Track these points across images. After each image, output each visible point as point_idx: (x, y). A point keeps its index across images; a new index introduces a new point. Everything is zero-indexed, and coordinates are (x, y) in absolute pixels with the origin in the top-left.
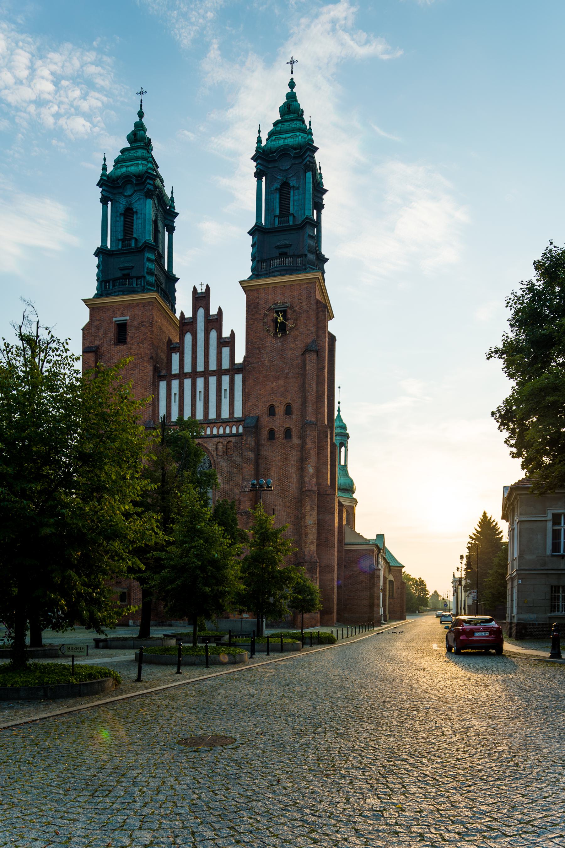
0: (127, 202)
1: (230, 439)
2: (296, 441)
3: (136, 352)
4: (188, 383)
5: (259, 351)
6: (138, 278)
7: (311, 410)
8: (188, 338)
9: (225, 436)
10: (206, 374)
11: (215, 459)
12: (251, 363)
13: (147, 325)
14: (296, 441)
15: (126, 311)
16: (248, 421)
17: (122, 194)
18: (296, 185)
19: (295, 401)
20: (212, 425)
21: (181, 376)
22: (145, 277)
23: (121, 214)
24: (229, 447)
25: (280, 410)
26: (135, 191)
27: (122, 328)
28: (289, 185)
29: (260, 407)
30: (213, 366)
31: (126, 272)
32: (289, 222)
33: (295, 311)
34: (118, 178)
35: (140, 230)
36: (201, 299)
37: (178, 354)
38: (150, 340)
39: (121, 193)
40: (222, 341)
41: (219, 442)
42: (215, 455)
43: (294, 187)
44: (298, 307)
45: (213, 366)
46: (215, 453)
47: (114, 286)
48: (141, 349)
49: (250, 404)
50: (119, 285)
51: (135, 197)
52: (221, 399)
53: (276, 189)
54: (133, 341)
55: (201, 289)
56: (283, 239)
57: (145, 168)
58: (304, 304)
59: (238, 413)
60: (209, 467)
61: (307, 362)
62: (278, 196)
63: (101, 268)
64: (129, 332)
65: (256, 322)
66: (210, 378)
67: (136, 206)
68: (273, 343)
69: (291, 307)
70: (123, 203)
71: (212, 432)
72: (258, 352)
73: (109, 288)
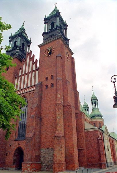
1: (33, 92)
2: (54, 87)
8: (24, 65)
18: (55, 22)
20: (28, 88)
21: (22, 75)
25: (49, 78)
42: (28, 98)
49: (40, 78)
59: (37, 83)
62: (51, 26)
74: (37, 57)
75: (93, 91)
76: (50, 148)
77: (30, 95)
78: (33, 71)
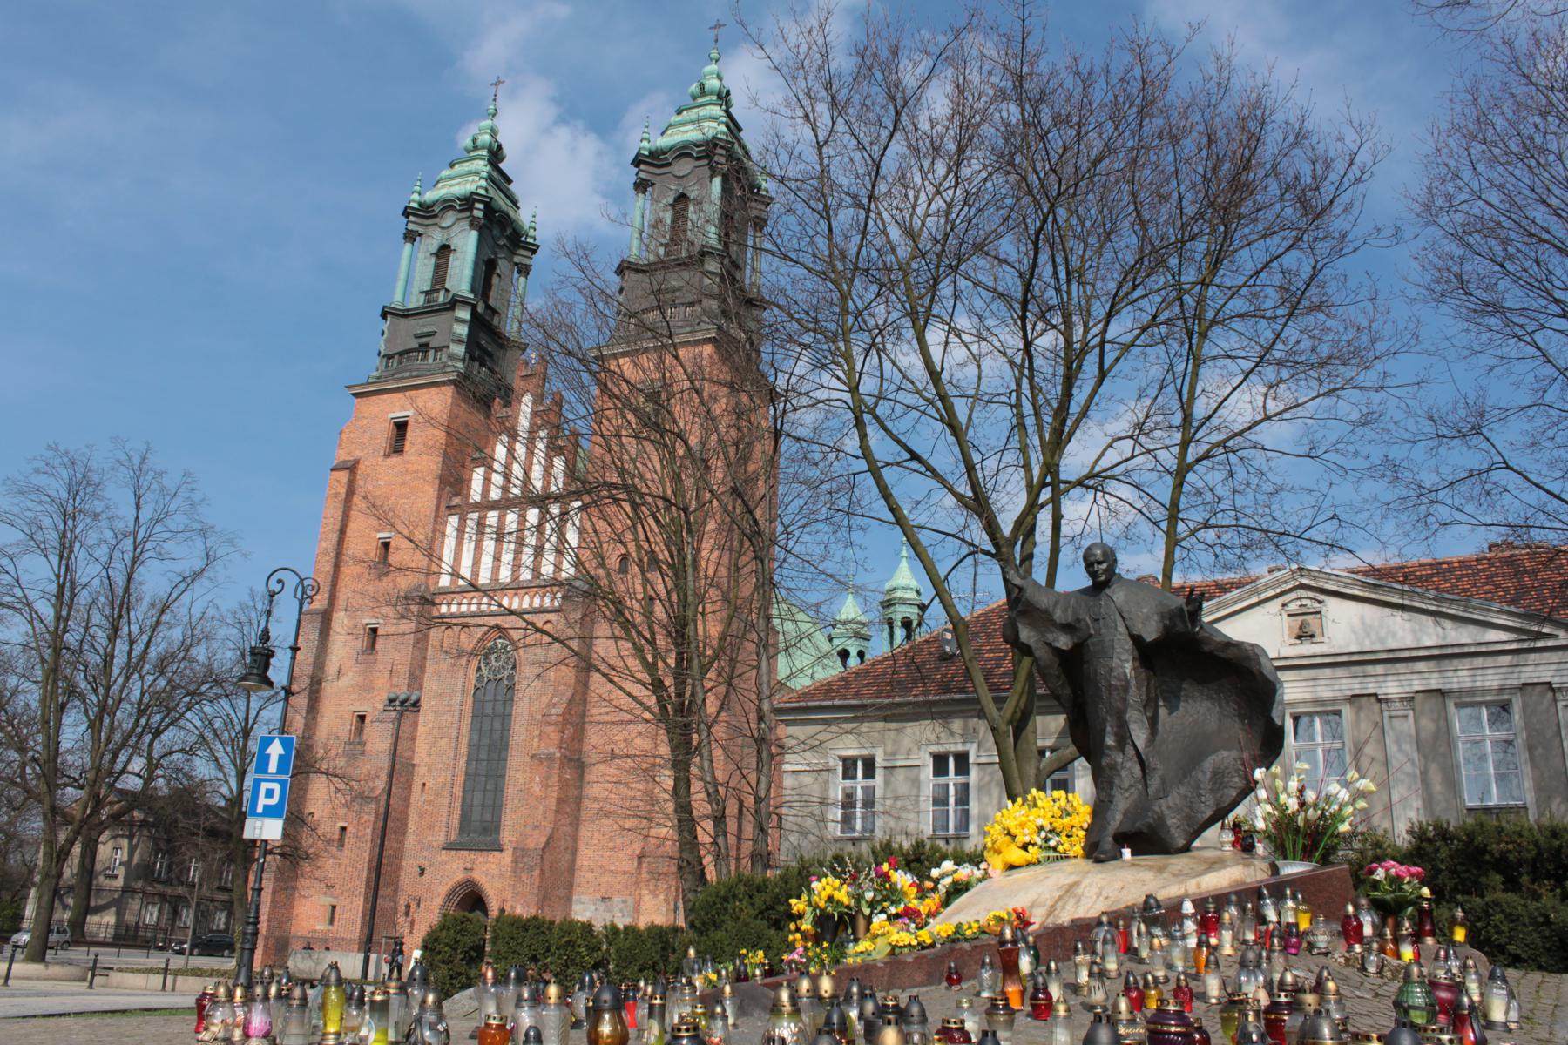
3: (416, 467)
6: (437, 350)
20: (522, 592)
27: (401, 427)
31: (424, 340)
34: (434, 203)
47: (400, 362)
57: (473, 188)
64: (410, 434)
67: (455, 243)
70: (433, 240)
76: (616, 899)
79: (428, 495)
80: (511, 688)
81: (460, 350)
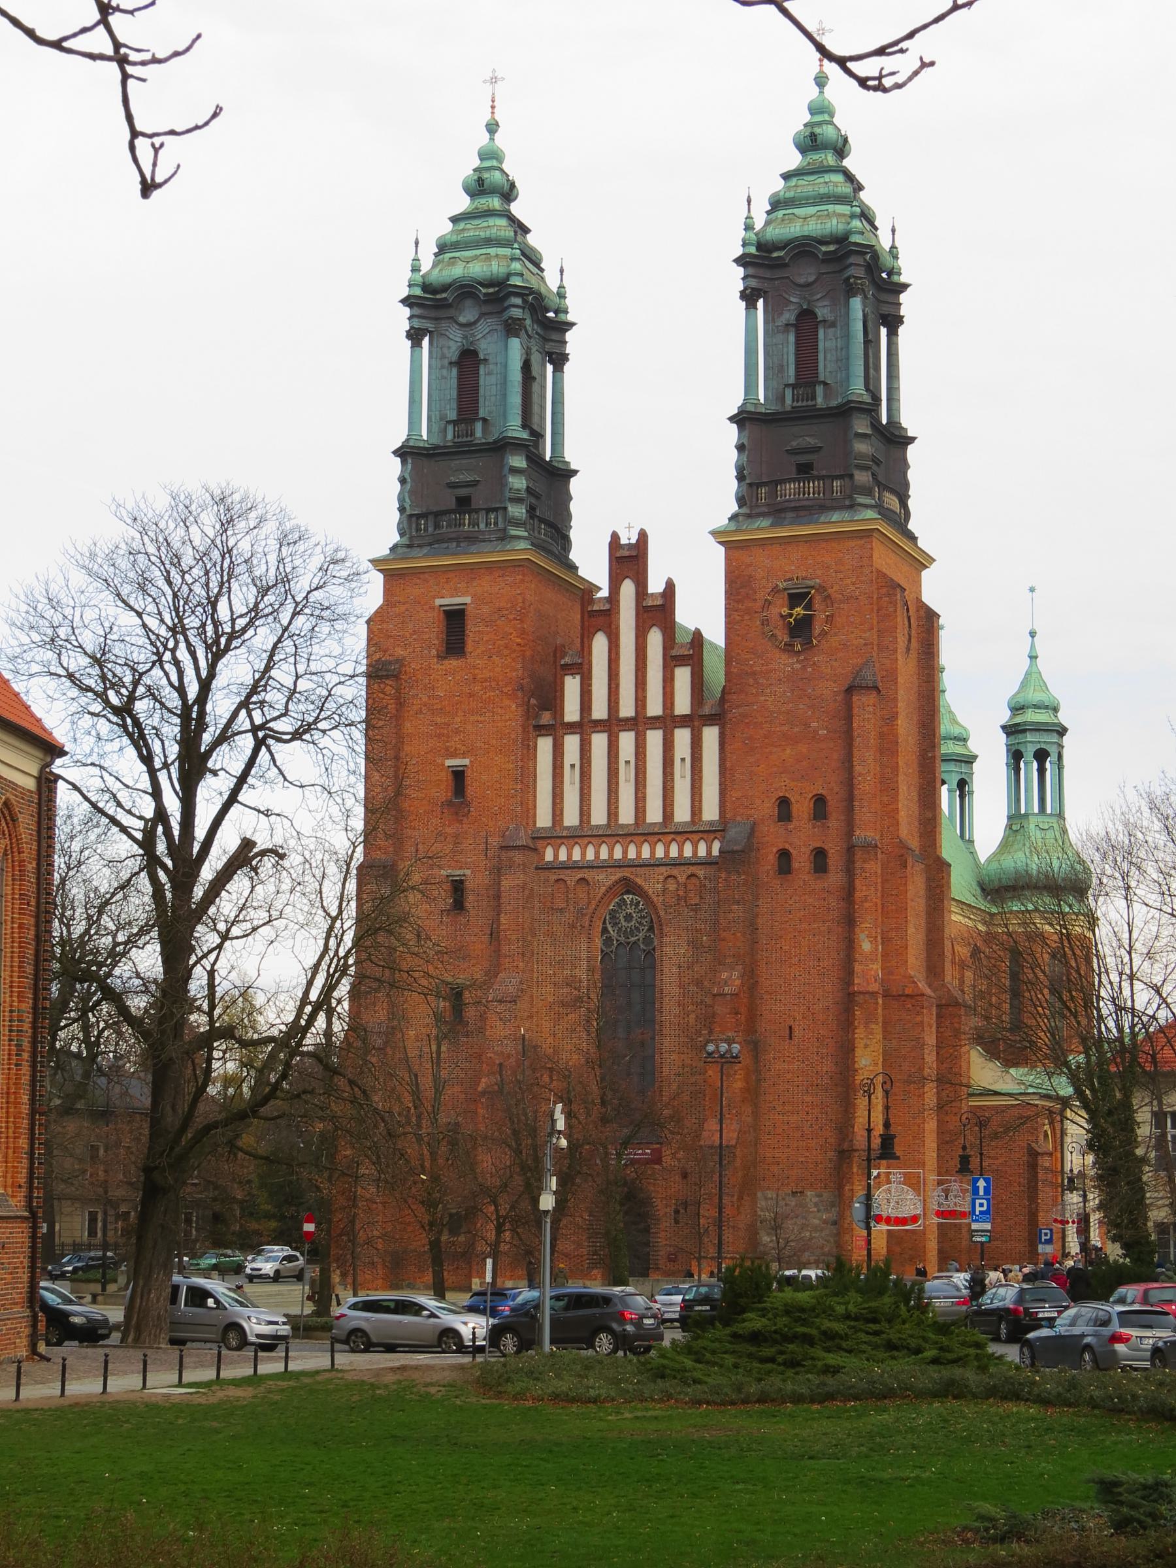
0: (465, 337)
2: (835, 877)
4: (599, 741)
5: (755, 680)
7: (865, 813)
8: (600, 644)
9: (680, 863)
10: (640, 723)
11: (662, 913)
12: (738, 706)
13: (511, 617)
14: (835, 877)
15: (463, 585)
16: (732, 833)
17: (453, 319)
19: (832, 790)
21: (585, 727)
22: (505, 509)
23: (451, 363)
24: (690, 887)
25: (802, 808)
26: (482, 315)
28: (815, 315)
29: (758, 801)
30: (654, 708)
31: (463, 492)
32: (814, 398)
33: (829, 596)
34: (445, 288)
35: (493, 398)
36: (629, 559)
37: (578, 677)
38: (518, 648)
39: (452, 318)
40: (674, 653)
41: (670, 876)
42: (659, 905)
43: (825, 321)
44: (836, 588)
45: (654, 708)
46: (661, 899)
47: (437, 526)
48: (498, 669)
50: (449, 526)
51: (483, 327)
52: (673, 780)
53: (787, 325)
54: (479, 651)
55: (628, 537)
56: (807, 437)
57: (503, 270)
58: (848, 581)
59: (711, 812)
60: (648, 930)
61: (855, 711)
62: (792, 338)
63: (408, 486)
64: (471, 630)
65: (747, 617)
66: (648, 732)
68: (784, 663)
69: (821, 589)
70: (455, 341)
71: (653, 852)
72: (751, 681)
73: (426, 530)
74: (703, 610)
75: (1033, 634)
77: (672, 886)
78: (668, 722)
79: (511, 712)
80: (650, 953)
81: (518, 511)
